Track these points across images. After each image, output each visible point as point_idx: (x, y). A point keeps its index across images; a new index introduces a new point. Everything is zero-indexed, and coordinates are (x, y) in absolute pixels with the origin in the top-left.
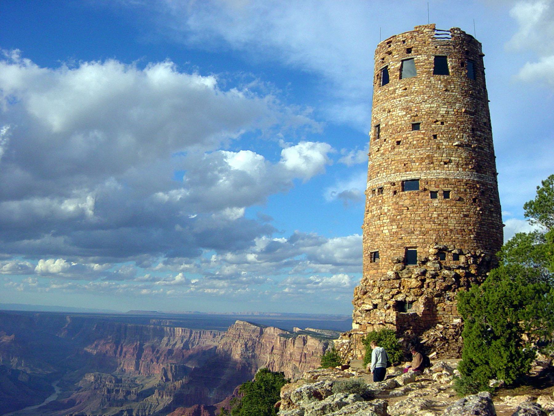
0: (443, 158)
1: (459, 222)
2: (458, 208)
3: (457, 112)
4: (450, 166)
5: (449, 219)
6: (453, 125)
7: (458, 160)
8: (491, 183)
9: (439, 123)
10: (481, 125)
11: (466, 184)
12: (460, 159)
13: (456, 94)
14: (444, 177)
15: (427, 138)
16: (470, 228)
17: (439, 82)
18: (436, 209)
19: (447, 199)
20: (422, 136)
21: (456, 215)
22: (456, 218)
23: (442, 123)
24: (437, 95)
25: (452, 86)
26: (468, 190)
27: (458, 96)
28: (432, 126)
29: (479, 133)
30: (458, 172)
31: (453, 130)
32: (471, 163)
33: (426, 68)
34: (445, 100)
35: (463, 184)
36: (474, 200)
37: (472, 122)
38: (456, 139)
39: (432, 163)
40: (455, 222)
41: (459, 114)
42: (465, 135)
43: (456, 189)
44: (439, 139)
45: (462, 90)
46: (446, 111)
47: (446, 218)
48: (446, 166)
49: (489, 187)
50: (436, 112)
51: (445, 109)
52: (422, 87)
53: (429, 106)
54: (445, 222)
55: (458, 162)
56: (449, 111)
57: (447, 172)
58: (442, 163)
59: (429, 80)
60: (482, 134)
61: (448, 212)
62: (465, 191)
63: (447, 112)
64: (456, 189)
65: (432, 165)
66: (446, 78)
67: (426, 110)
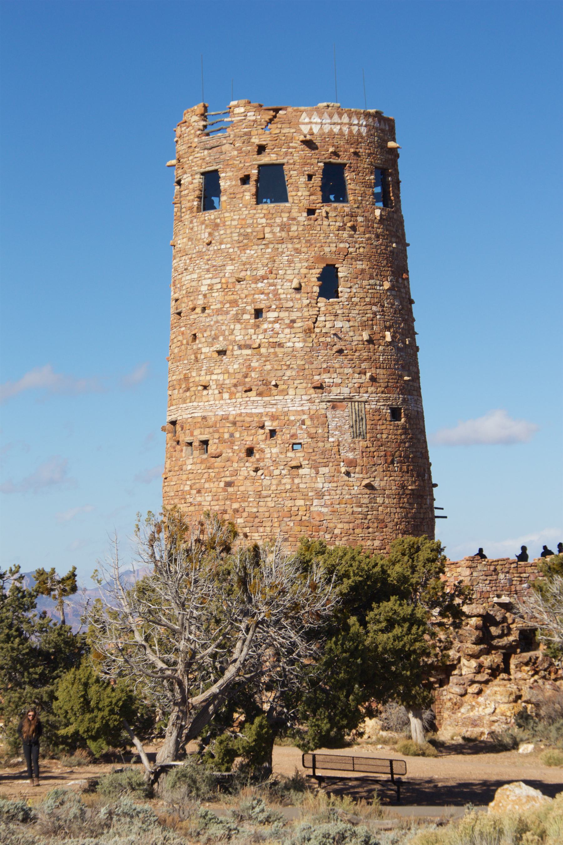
0: (201, 378)
1: (216, 498)
2: (217, 470)
3: (227, 283)
4: (210, 392)
5: (203, 491)
6: (219, 312)
7: (221, 379)
8: (300, 409)
9: (198, 310)
10: (282, 296)
11: (234, 423)
12: (226, 376)
13: (229, 246)
14: (199, 415)
15: (185, 342)
16: (235, 506)
17: (203, 227)
18: (190, 475)
19: (205, 456)
20: (180, 338)
21: (212, 485)
22: (214, 490)
23: (204, 309)
24: (201, 254)
25: (222, 232)
26: (237, 435)
27: (231, 250)
28: (192, 317)
29: (271, 315)
30: (222, 402)
31: (217, 322)
32: (247, 380)
33: (189, 201)
34: (209, 262)
35: (228, 425)
36: (250, 452)
37: (256, 296)
38: (221, 338)
39: (188, 390)
40: (209, 498)
41: (229, 286)
42: (238, 326)
43: (216, 435)
44: (197, 341)
45: (240, 235)
46: (209, 285)
47: (199, 492)
48: (205, 392)
49: (292, 418)
50: (196, 291)
51: (209, 282)
52: (185, 240)
53: (188, 277)
54: (199, 499)
55: (221, 382)
56: (213, 284)
57: (206, 404)
58: (200, 388)
59: (191, 225)
60: (283, 314)
61: (203, 481)
62: (232, 435)
63: (211, 287)
64: (216, 435)
65: (188, 394)
66: (213, 217)
67: (188, 286)
